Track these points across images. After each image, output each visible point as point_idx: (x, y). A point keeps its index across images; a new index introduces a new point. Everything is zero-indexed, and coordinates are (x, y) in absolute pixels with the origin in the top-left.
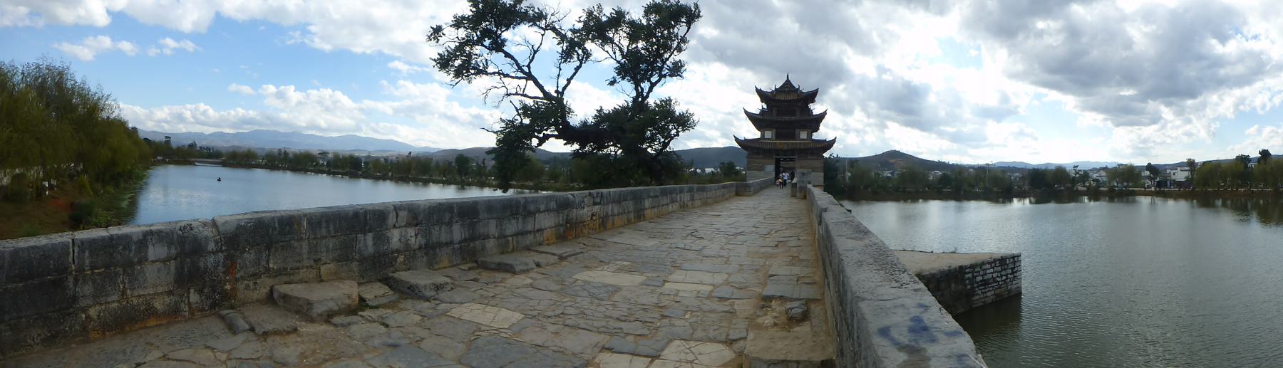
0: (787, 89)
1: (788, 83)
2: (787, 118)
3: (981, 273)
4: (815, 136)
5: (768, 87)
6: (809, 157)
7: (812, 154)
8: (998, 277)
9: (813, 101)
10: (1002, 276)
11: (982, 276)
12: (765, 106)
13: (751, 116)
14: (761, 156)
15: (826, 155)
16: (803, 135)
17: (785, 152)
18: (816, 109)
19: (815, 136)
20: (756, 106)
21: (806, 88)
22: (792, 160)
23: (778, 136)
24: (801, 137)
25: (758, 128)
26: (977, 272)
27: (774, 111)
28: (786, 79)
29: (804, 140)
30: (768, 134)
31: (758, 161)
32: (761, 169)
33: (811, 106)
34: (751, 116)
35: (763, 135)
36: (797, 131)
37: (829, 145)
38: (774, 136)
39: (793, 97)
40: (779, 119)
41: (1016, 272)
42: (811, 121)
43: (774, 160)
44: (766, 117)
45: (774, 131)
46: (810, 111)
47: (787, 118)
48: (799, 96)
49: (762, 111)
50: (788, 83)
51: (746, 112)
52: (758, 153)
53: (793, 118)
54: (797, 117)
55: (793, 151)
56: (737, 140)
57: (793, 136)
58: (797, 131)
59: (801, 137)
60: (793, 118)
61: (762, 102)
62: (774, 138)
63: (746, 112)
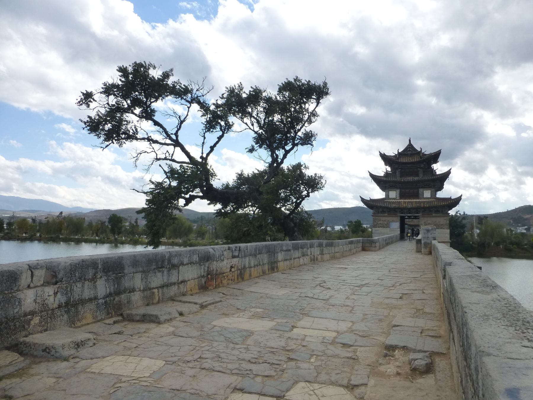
0: (409, 152)
1: (410, 147)
2: (410, 179)
4: (440, 194)
5: (391, 152)
6: (434, 215)
7: (437, 211)
9: (436, 162)
12: (389, 169)
13: (375, 178)
15: (452, 212)
16: (427, 194)
17: (409, 210)
18: (439, 168)
19: (440, 194)
21: (428, 150)
22: (416, 218)
23: (402, 196)
24: (425, 196)
27: (397, 174)
28: (408, 143)
30: (393, 194)
31: (384, 218)
32: (387, 226)
33: (435, 166)
34: (375, 178)
35: (387, 195)
36: (421, 190)
39: (416, 159)
40: (404, 179)
42: (434, 181)
43: (399, 218)
44: (389, 179)
45: (398, 191)
47: (410, 179)
48: (421, 158)
49: (387, 174)
50: (410, 147)
51: (372, 176)
52: (383, 212)
53: (416, 178)
54: (421, 177)
55: (417, 210)
56: (363, 200)
57: (417, 196)
58: (421, 190)
59: (425, 196)
60: (416, 178)
61: (386, 165)
62: (398, 198)
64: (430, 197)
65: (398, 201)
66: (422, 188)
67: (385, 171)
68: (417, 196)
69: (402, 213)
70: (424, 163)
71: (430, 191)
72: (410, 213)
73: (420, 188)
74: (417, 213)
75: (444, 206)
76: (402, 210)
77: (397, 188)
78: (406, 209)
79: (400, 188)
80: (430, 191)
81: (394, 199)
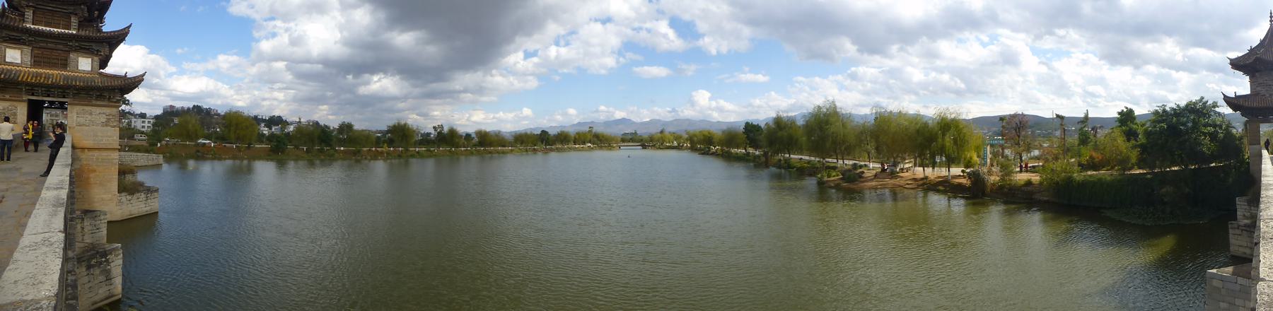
7: (100, 97)
16: (85, 64)
22: (62, 106)
23: (36, 62)
37: (132, 83)
38: (28, 59)
46: (100, 31)
57: (64, 65)
64: (90, 69)
65: (27, 70)
66: (76, 51)
68: (64, 65)
69: (33, 95)
70: (82, 7)
71: (90, 60)
72: (49, 96)
74: (64, 97)
75: (112, 90)
76: (31, 88)
78: (42, 87)
80: (90, 60)
81: (17, 65)
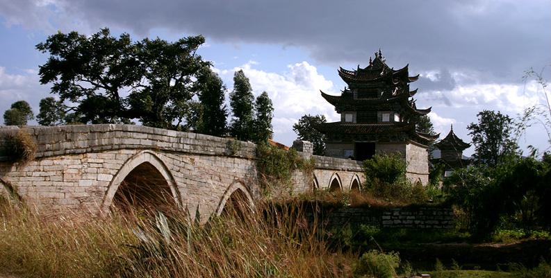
1: (377, 64)
3: (400, 217)
5: (351, 67)
8: (420, 224)
10: (425, 224)
11: (401, 220)
14: (341, 141)
20: (338, 88)
23: (359, 120)
24: (383, 121)
25: (339, 110)
26: (396, 216)
29: (386, 122)
30: (349, 118)
36: (379, 114)
38: (355, 119)
41: (447, 224)
45: (355, 115)
49: (345, 93)
51: (324, 95)
59: (383, 121)
62: (355, 122)
63: (324, 95)
66: (381, 110)
67: (344, 90)
73: (377, 110)
77: (353, 110)
79: (357, 110)
